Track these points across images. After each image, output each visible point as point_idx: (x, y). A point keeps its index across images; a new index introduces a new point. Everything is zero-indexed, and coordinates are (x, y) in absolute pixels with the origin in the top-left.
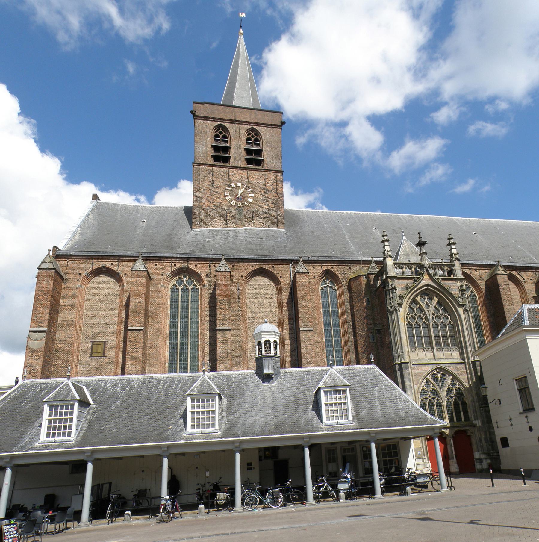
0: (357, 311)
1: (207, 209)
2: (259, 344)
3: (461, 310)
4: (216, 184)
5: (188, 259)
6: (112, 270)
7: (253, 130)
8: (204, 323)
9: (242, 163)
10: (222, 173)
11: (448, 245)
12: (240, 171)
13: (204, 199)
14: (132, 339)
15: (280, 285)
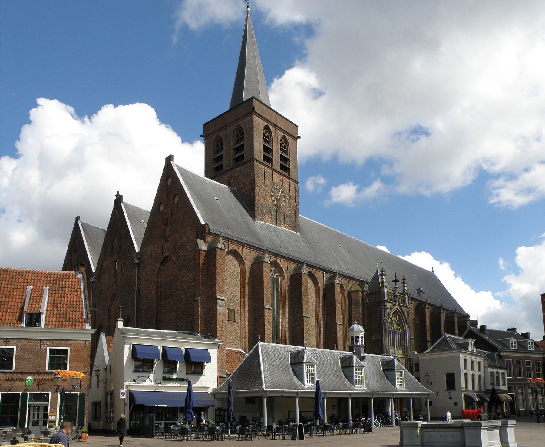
0: (354, 314)
1: (262, 204)
2: (352, 337)
3: (407, 326)
4: (267, 183)
5: (277, 255)
6: (238, 253)
7: (284, 137)
8: (285, 307)
9: (278, 168)
10: (269, 174)
11: (393, 281)
12: (278, 175)
13: (260, 195)
14: (267, 315)
15: (319, 287)
